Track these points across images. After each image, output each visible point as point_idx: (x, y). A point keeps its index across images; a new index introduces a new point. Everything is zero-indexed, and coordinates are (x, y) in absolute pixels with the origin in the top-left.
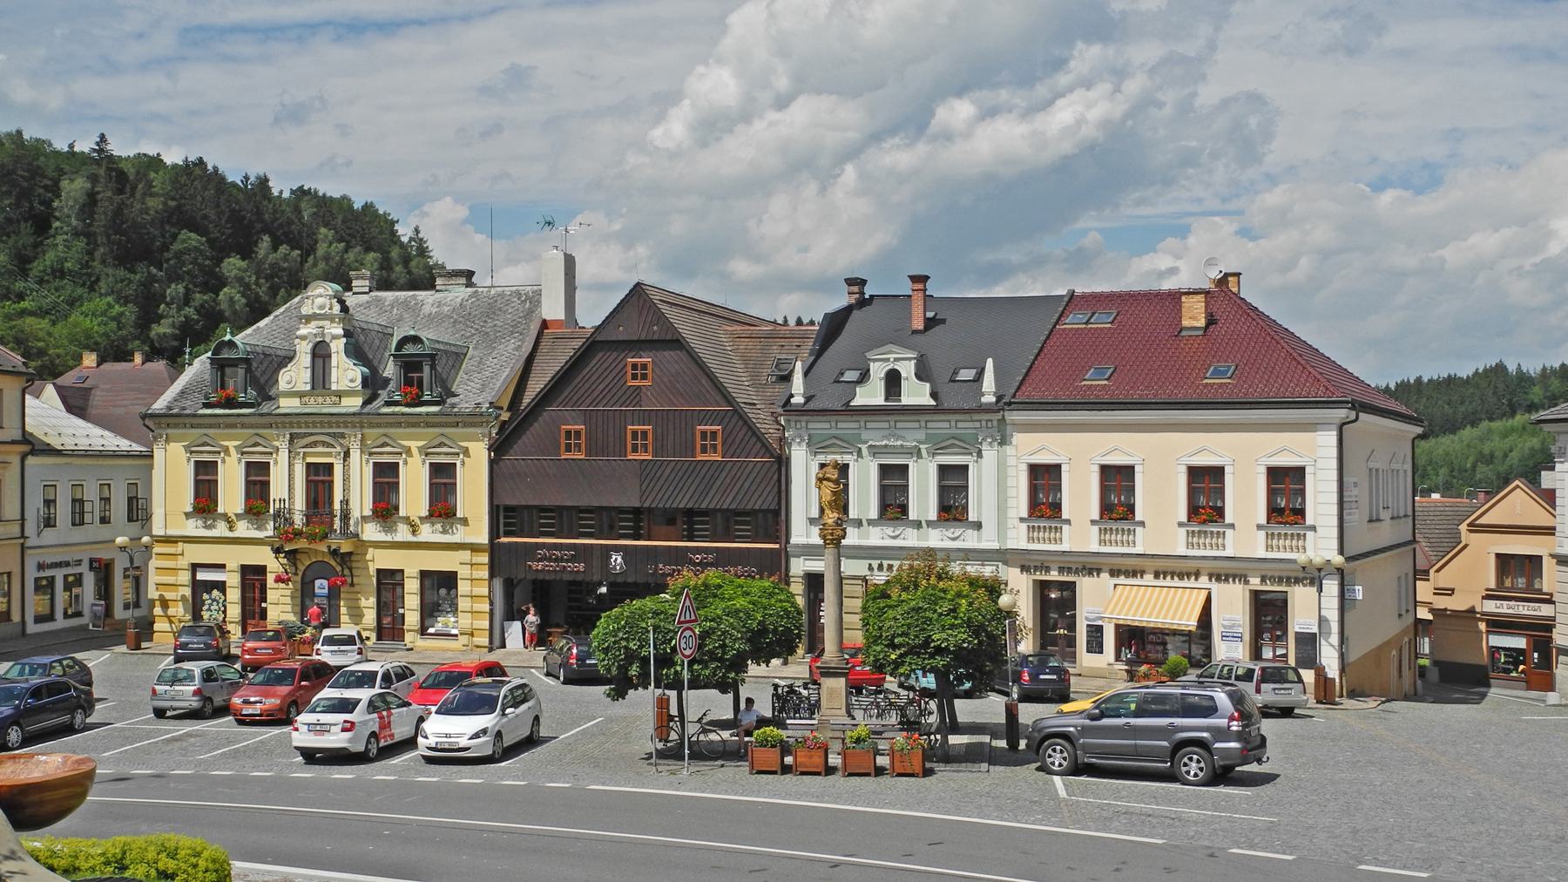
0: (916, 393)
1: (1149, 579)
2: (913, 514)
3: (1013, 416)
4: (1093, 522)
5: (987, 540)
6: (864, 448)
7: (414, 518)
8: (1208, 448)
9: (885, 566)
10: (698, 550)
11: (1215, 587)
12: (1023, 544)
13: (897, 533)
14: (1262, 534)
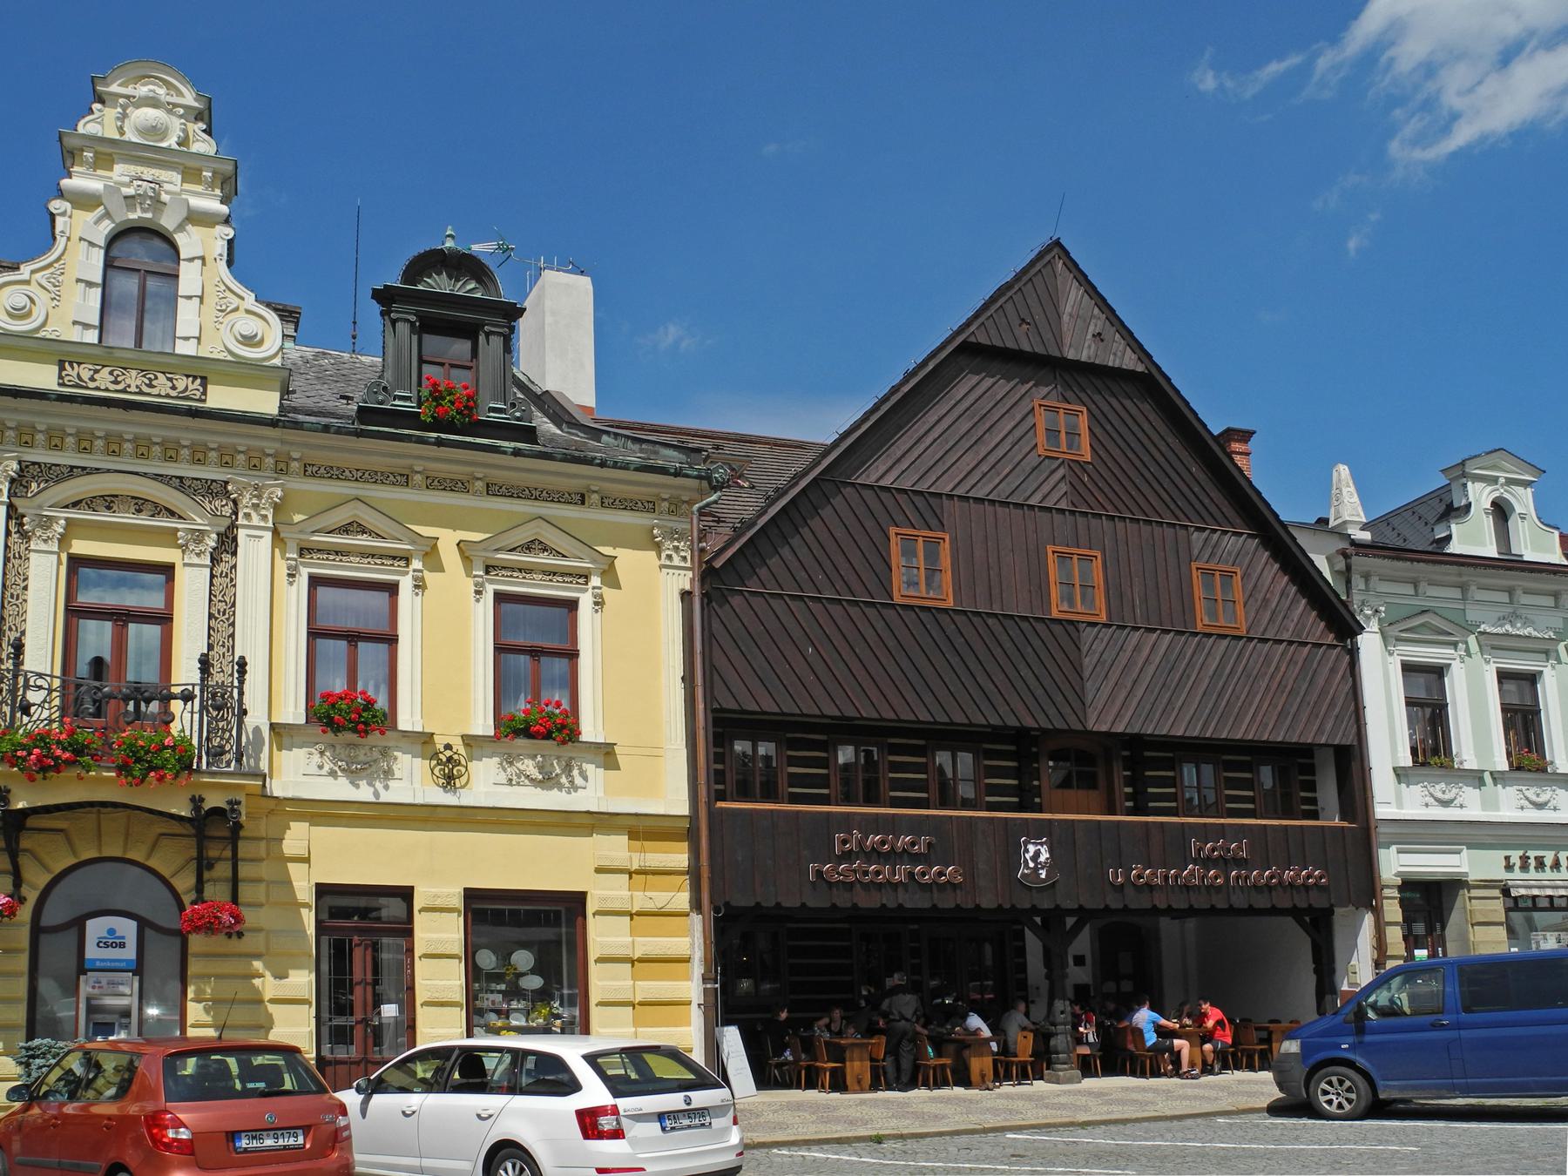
7: (447, 734)
9: (1532, 862)
10: (1205, 833)
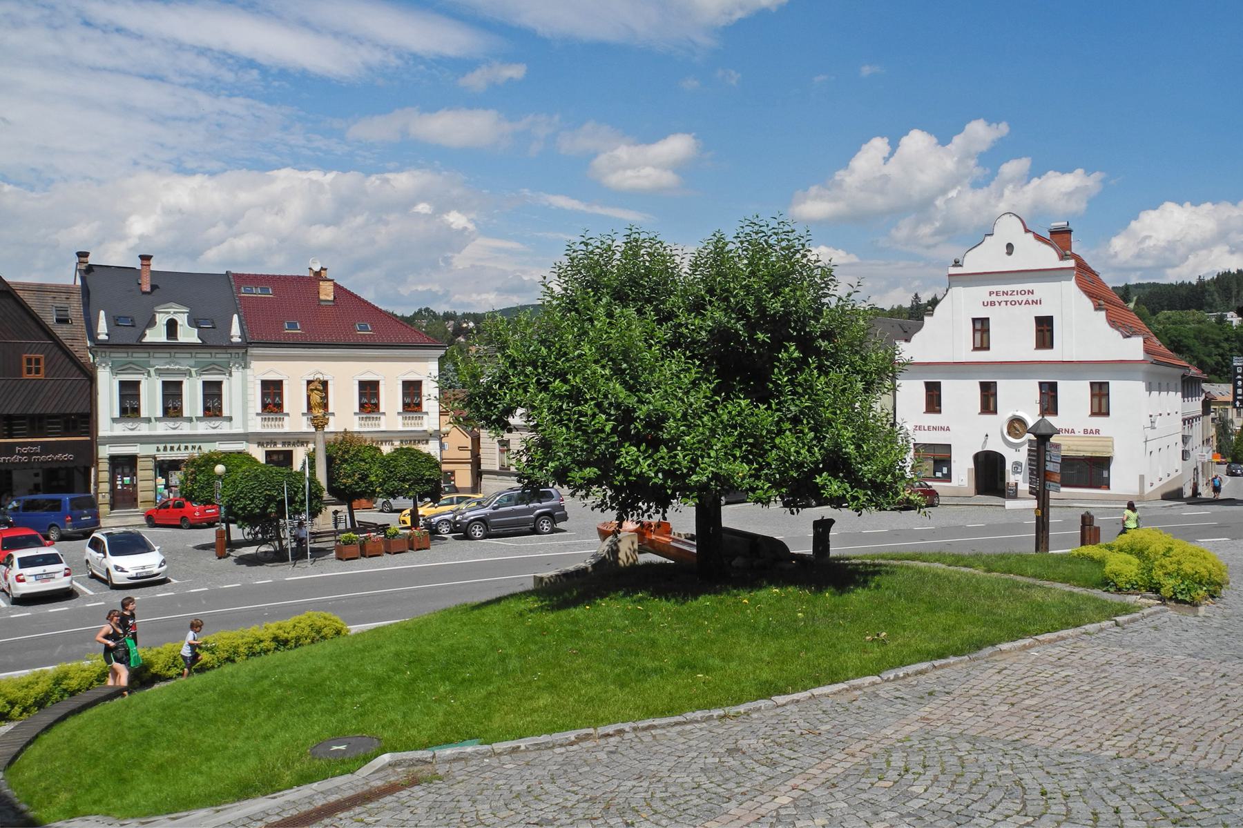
0: (187, 334)
2: (186, 413)
3: (254, 351)
5: (236, 428)
6: (152, 370)
9: (169, 448)
12: (259, 429)
13: (177, 426)
14: (400, 417)
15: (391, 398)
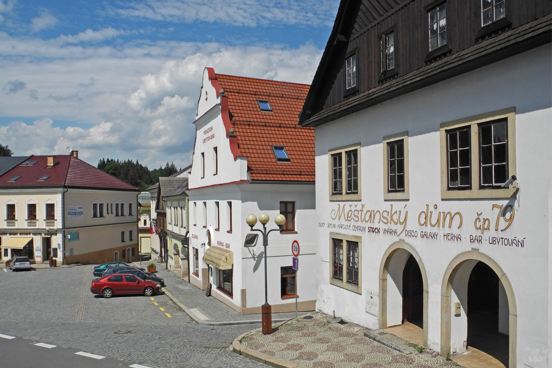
1: (19, 235)
4: (5, 220)
8: (33, 199)
11: (34, 237)
15: (41, 213)
